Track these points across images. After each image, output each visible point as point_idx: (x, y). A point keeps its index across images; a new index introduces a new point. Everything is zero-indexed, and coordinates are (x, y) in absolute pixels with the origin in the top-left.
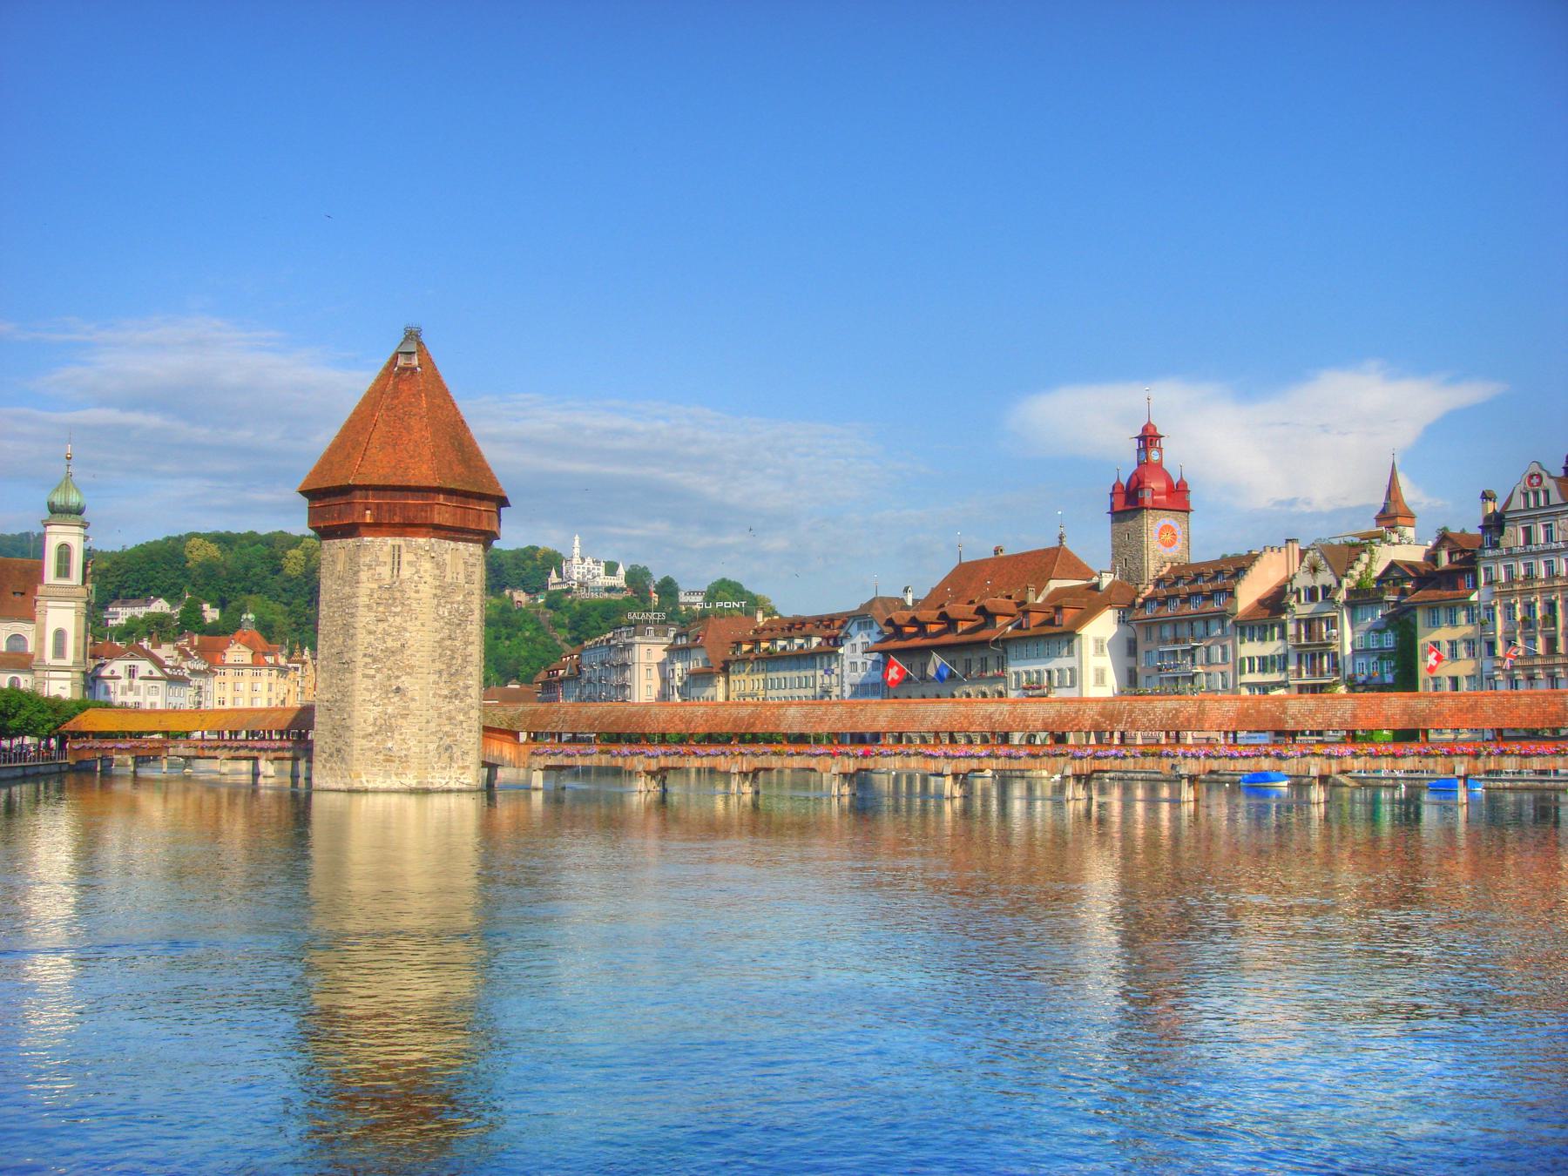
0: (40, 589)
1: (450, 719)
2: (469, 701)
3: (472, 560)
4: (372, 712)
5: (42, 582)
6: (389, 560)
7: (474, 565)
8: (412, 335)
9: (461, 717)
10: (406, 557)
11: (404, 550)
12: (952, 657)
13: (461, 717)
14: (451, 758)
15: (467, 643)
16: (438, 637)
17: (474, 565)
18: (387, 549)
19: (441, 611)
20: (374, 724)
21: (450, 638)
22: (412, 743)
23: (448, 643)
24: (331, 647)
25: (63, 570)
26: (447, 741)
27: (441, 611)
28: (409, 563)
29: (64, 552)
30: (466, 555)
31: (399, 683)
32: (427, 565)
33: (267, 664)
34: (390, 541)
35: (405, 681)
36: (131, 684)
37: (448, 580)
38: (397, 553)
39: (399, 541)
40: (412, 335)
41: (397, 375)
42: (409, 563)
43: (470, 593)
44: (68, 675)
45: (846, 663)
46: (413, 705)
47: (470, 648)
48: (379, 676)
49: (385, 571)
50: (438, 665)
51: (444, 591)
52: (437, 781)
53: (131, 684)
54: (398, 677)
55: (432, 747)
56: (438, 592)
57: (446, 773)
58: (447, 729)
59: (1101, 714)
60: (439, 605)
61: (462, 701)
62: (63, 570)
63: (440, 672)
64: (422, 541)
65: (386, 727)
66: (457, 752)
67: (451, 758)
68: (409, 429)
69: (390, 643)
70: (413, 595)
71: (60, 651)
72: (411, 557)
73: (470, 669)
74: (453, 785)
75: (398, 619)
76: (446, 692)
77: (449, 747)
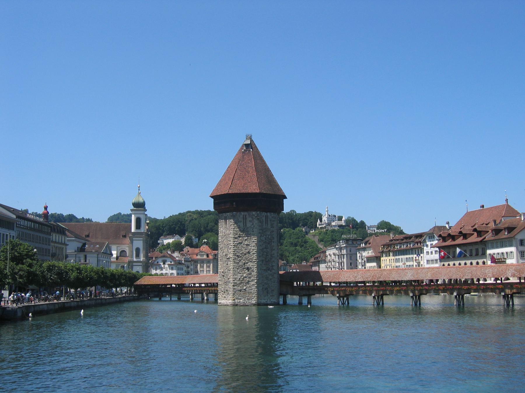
2: (273, 271)
4: (239, 276)
6: (242, 220)
9: (271, 277)
10: (249, 219)
11: (247, 216)
12: (465, 248)
13: (271, 277)
16: (261, 248)
18: (241, 216)
20: (239, 280)
21: (266, 248)
23: (265, 250)
24: (223, 253)
28: (250, 221)
31: (247, 265)
32: (256, 222)
34: (242, 213)
35: (250, 265)
37: (264, 226)
38: (245, 218)
39: (246, 213)
41: (243, 153)
42: (250, 221)
43: (272, 231)
44: (141, 264)
45: (425, 252)
48: (240, 264)
54: (247, 263)
56: (261, 231)
58: (266, 281)
59: (515, 270)
60: (261, 236)
61: (271, 271)
63: (262, 261)
64: (254, 213)
67: (268, 293)
68: (248, 172)
70: (252, 233)
71: (138, 255)
72: (250, 219)
76: (265, 268)
77: (266, 289)
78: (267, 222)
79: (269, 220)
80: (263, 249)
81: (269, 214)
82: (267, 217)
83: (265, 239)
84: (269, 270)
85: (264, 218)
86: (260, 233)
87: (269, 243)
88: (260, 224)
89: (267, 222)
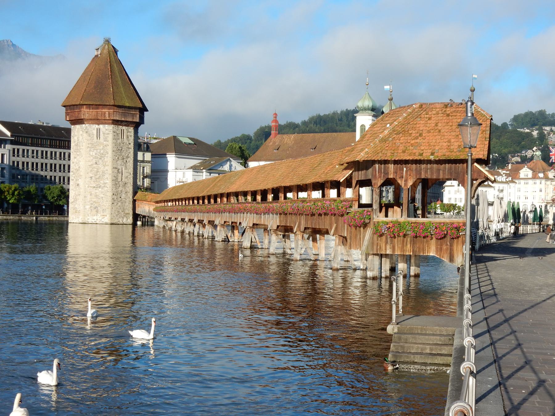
2: (106, 189)
3: (107, 132)
7: (108, 134)
14: (97, 211)
17: (108, 134)
19: (91, 153)
22: (81, 205)
26: (96, 205)
27: (91, 154)
30: (104, 130)
31: (78, 182)
32: (85, 135)
33: (539, 178)
36: (458, 190)
42: (81, 135)
46: (81, 190)
47: (106, 168)
53: (458, 190)
55: (88, 207)
56: (90, 146)
57: (95, 218)
58: (94, 200)
63: (91, 177)
65: (75, 200)
67: (97, 211)
69: (77, 167)
73: (107, 176)
75: (78, 157)
78: (98, 136)
79: (101, 133)
80: (92, 165)
81: (101, 126)
82: (98, 131)
83: (96, 154)
84: (100, 187)
87: (100, 158)
88: (90, 138)
89: (98, 136)
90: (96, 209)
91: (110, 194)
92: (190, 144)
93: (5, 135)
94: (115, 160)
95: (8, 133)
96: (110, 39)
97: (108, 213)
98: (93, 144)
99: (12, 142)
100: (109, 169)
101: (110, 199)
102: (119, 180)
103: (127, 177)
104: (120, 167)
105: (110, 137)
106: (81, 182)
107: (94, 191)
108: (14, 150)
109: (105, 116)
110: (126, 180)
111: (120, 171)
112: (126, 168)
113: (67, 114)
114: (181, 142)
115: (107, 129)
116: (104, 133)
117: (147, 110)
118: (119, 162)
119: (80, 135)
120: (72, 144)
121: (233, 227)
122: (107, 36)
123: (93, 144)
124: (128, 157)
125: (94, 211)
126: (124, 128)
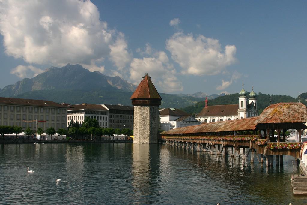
0: (238, 110)
1: (144, 133)
5: (239, 108)
8: (147, 75)
10: (138, 109)
13: (146, 132)
14: (144, 139)
15: (147, 121)
23: (143, 121)
25: (242, 106)
29: (242, 102)
32: (139, 110)
34: (136, 107)
40: (147, 75)
49: (136, 111)
50: (141, 125)
51: (142, 114)
52: (142, 142)
57: (143, 141)
60: (141, 115)
62: (242, 106)
65: (136, 134)
66: (145, 138)
67: (144, 139)
73: (147, 125)
74: (145, 143)
77: (144, 137)
78: (144, 110)
80: (142, 121)
85: (143, 108)
86: (140, 114)
89: (144, 110)
90: (144, 138)
91: (149, 132)
92: (175, 111)
93: (107, 110)
94: (150, 119)
95: (108, 109)
96: (147, 73)
97: (148, 139)
98: (142, 113)
99: (109, 113)
100: (148, 122)
101: (149, 134)
102: (152, 126)
103: (155, 125)
104: (152, 121)
105: (149, 110)
106: (138, 127)
107: (143, 131)
108: (110, 115)
109: (147, 103)
110: (155, 126)
111: (153, 123)
112: (155, 122)
113: (132, 102)
114: (171, 110)
115: (147, 108)
116: (146, 109)
117: (162, 100)
118: (152, 120)
119: (137, 110)
120: (134, 113)
121: (204, 145)
122: (147, 72)
123: (142, 113)
124: (155, 118)
125: (143, 139)
126: (154, 107)
